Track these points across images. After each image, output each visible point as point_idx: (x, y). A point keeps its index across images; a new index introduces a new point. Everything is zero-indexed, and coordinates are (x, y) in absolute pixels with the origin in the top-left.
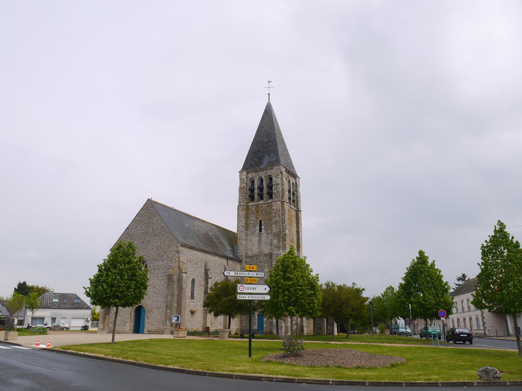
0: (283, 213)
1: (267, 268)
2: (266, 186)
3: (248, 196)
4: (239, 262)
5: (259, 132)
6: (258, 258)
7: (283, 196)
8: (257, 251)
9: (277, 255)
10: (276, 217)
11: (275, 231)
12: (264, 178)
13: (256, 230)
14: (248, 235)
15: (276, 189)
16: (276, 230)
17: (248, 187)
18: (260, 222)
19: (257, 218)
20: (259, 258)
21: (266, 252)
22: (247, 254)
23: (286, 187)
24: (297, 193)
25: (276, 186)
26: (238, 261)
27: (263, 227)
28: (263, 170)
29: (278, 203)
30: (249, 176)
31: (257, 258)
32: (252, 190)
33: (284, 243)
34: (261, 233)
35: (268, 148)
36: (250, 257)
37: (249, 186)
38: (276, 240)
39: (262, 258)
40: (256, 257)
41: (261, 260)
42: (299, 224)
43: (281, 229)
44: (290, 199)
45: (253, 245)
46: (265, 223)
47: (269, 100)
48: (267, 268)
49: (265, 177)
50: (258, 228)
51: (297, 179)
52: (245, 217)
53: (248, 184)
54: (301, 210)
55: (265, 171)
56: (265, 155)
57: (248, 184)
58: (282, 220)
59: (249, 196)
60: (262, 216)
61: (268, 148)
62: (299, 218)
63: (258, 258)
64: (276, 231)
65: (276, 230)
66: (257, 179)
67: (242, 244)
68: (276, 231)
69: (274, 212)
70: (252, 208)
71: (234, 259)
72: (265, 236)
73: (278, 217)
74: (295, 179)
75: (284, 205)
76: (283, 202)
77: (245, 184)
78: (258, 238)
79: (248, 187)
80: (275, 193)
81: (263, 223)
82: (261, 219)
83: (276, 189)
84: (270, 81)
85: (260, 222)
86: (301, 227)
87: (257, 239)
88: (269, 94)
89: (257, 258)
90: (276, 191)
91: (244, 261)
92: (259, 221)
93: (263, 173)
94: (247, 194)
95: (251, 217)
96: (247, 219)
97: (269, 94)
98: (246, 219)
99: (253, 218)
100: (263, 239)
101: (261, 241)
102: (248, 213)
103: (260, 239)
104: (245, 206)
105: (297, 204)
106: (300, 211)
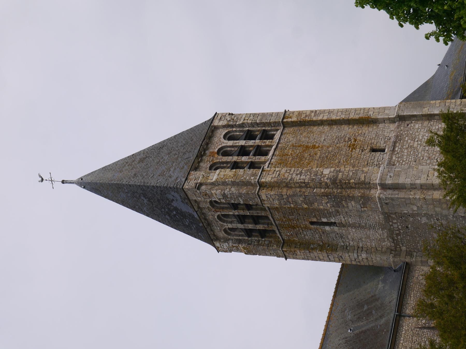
0: (284, 185)
1: (420, 219)
2: (233, 211)
3: (263, 239)
4: (409, 268)
5: (135, 207)
6: (397, 232)
7: (247, 184)
8: (380, 231)
9: (384, 204)
10: (296, 202)
11: (328, 204)
12: (219, 213)
13: (333, 232)
14: (348, 244)
15: (235, 198)
16: (326, 203)
17: (244, 238)
18: (312, 223)
19: (306, 228)
20: (398, 230)
21: (380, 217)
22: (390, 250)
23: (228, 173)
24: (246, 124)
25: (228, 198)
26: (406, 275)
27: (325, 220)
28: (203, 214)
29: (264, 197)
30: (222, 235)
31: (397, 235)
32: (249, 233)
33: (353, 186)
34: (339, 223)
35: (158, 200)
36: (396, 244)
37: (242, 236)
38: (349, 204)
39: (395, 226)
40: (395, 236)
41: (400, 227)
42: (313, 121)
43: (323, 190)
44: (252, 165)
45: (368, 237)
46: (315, 216)
47: (73, 183)
48: (420, 219)
49: (217, 212)
50: (327, 228)
51: (216, 123)
52: (308, 251)
53: (238, 238)
54: (283, 111)
55: (204, 211)
56: (173, 206)
57: (238, 238)
58: (300, 187)
59: (262, 238)
60: (300, 221)
61: (158, 200)
62: (300, 121)
63: (397, 232)
64: (328, 202)
65: (326, 203)
66: (225, 224)
67: (367, 259)
68: (328, 202)
69: (285, 204)
70: (286, 235)
71: (403, 292)
72: (344, 217)
73: (295, 198)
74: (216, 128)
75: (266, 182)
76: (262, 185)
77: (239, 246)
78: (350, 229)
79: (244, 238)
80: (243, 201)
81: (315, 220)
82: (307, 223)
83: (235, 198)
84: (40, 179)
85: (312, 223)
86: (323, 112)
87: (354, 230)
88: (63, 182)
89: (397, 235)
90: (240, 198)
91: (408, 260)
92: (313, 226)
93: (210, 214)
94: (259, 241)
95: (307, 237)
96: (313, 244)
97: (63, 182)
98: (312, 246)
99: (308, 236)
100: (351, 221)
101: (358, 225)
102: (299, 242)
103: (353, 226)
104: (283, 249)
105: (269, 124)
106: (283, 119)
